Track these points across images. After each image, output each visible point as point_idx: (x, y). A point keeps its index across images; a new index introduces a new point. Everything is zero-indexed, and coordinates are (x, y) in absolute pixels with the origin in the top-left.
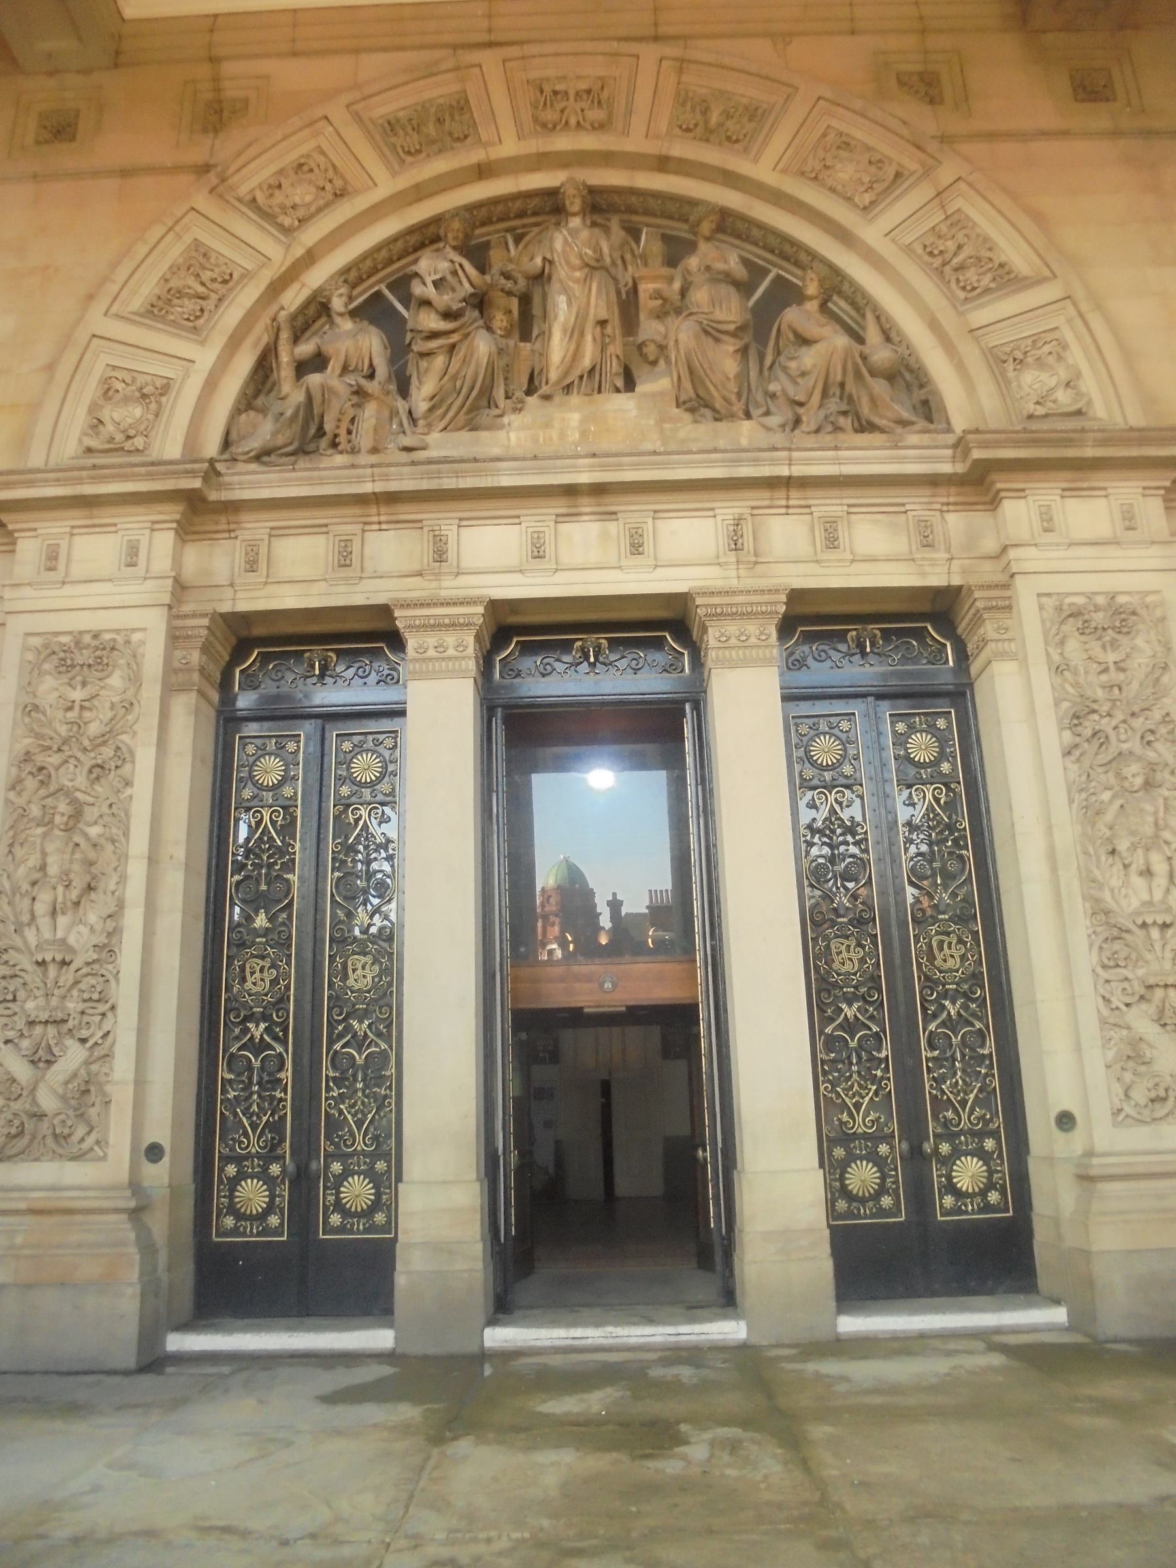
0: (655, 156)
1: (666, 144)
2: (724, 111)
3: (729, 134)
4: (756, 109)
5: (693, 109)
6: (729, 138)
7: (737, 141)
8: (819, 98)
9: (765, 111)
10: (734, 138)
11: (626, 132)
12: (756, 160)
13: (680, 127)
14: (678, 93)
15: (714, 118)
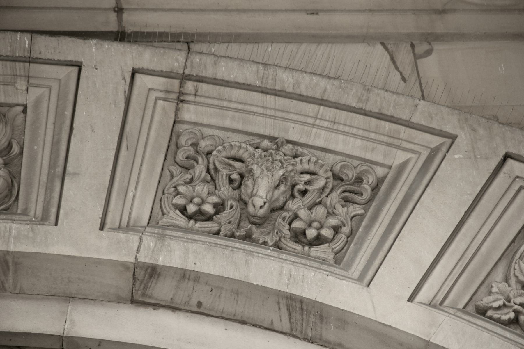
0: (124, 266)
1: (149, 242)
2: (283, 180)
3: (297, 224)
4: (359, 180)
5: (212, 173)
6: (299, 236)
7: (319, 240)
8: (507, 157)
9: (380, 182)
10: (311, 233)
11: (50, 215)
12: (366, 279)
13: (183, 210)
14: (173, 143)
15: (262, 191)
